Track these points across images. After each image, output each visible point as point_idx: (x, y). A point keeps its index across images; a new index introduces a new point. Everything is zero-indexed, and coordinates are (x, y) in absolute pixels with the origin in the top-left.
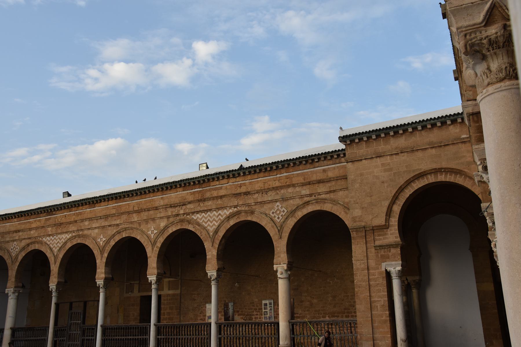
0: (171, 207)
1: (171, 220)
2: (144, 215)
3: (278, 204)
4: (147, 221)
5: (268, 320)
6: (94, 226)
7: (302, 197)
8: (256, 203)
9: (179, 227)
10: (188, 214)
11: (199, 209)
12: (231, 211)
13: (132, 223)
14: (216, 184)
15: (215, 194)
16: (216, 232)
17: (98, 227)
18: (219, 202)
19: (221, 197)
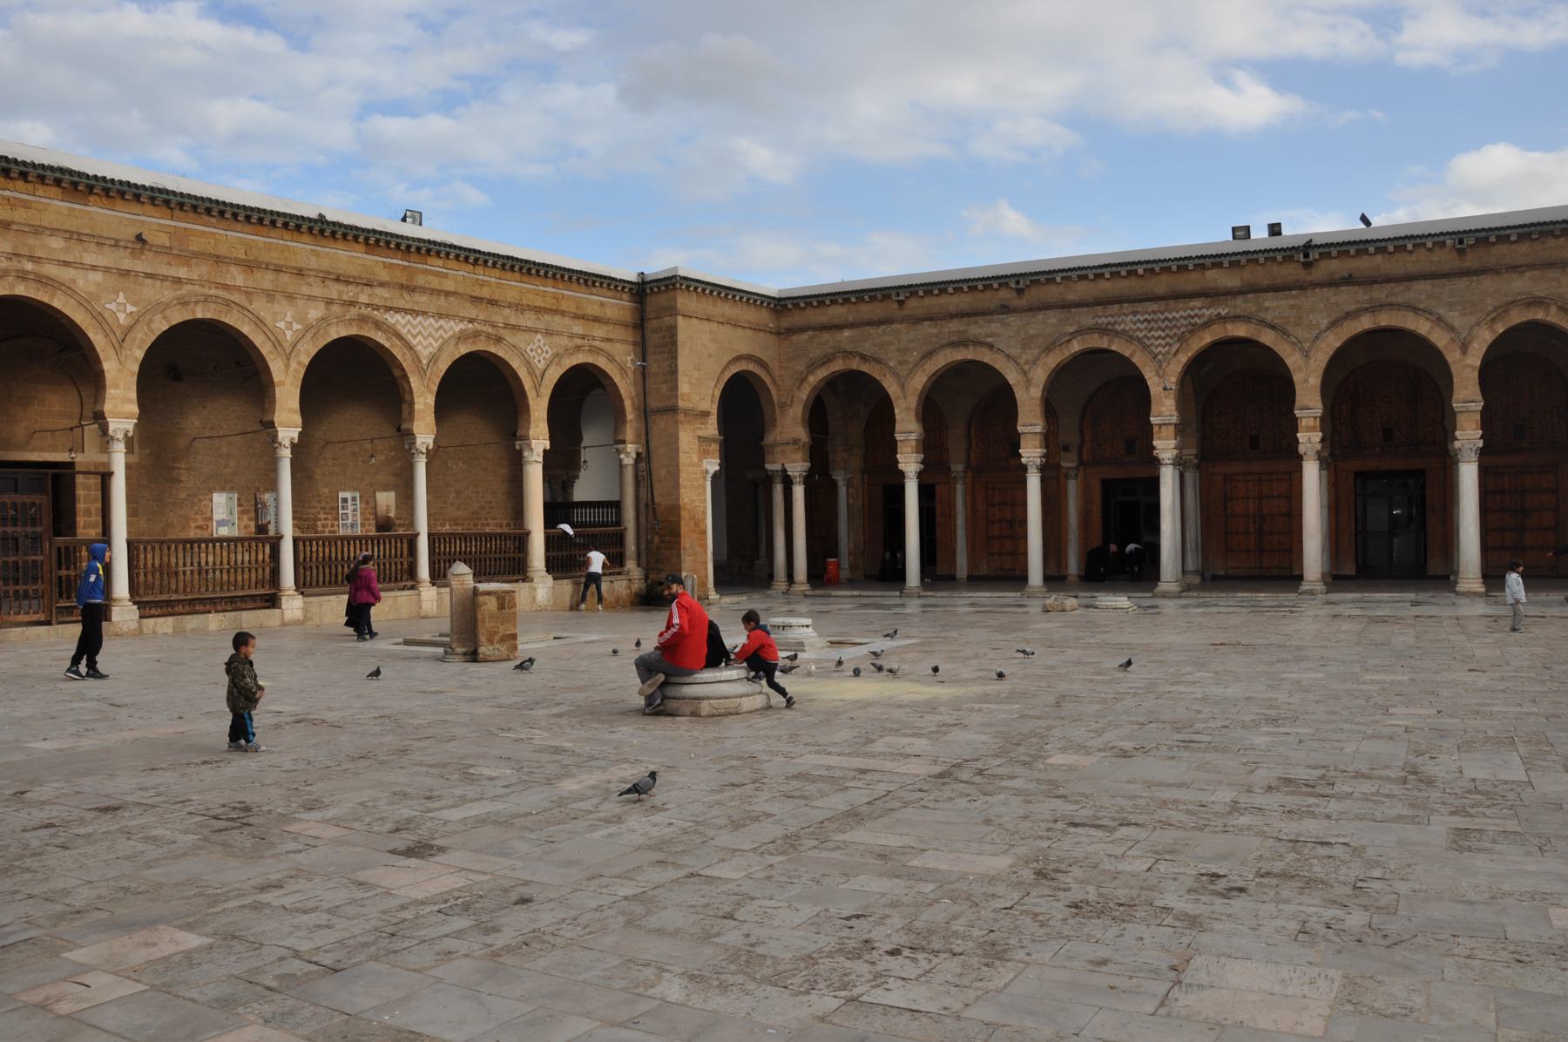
0: (338, 280)
1: (335, 308)
2: (266, 280)
3: (539, 336)
4: (270, 296)
5: (349, 532)
6: (89, 259)
7: (572, 336)
8: (506, 326)
9: (354, 331)
10: (377, 308)
11: (401, 304)
12: (462, 326)
13: (226, 287)
14: (436, 265)
15: (435, 283)
16: (434, 359)
17: (107, 270)
18: (442, 301)
19: (448, 294)
